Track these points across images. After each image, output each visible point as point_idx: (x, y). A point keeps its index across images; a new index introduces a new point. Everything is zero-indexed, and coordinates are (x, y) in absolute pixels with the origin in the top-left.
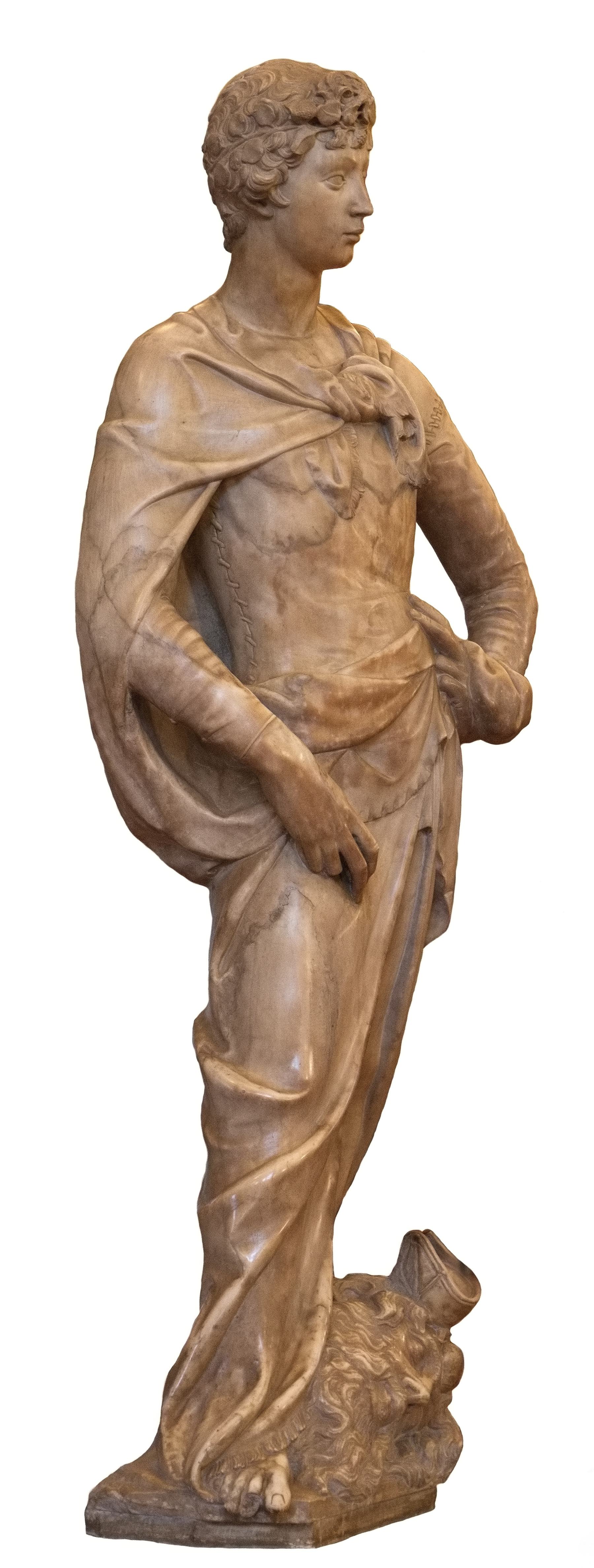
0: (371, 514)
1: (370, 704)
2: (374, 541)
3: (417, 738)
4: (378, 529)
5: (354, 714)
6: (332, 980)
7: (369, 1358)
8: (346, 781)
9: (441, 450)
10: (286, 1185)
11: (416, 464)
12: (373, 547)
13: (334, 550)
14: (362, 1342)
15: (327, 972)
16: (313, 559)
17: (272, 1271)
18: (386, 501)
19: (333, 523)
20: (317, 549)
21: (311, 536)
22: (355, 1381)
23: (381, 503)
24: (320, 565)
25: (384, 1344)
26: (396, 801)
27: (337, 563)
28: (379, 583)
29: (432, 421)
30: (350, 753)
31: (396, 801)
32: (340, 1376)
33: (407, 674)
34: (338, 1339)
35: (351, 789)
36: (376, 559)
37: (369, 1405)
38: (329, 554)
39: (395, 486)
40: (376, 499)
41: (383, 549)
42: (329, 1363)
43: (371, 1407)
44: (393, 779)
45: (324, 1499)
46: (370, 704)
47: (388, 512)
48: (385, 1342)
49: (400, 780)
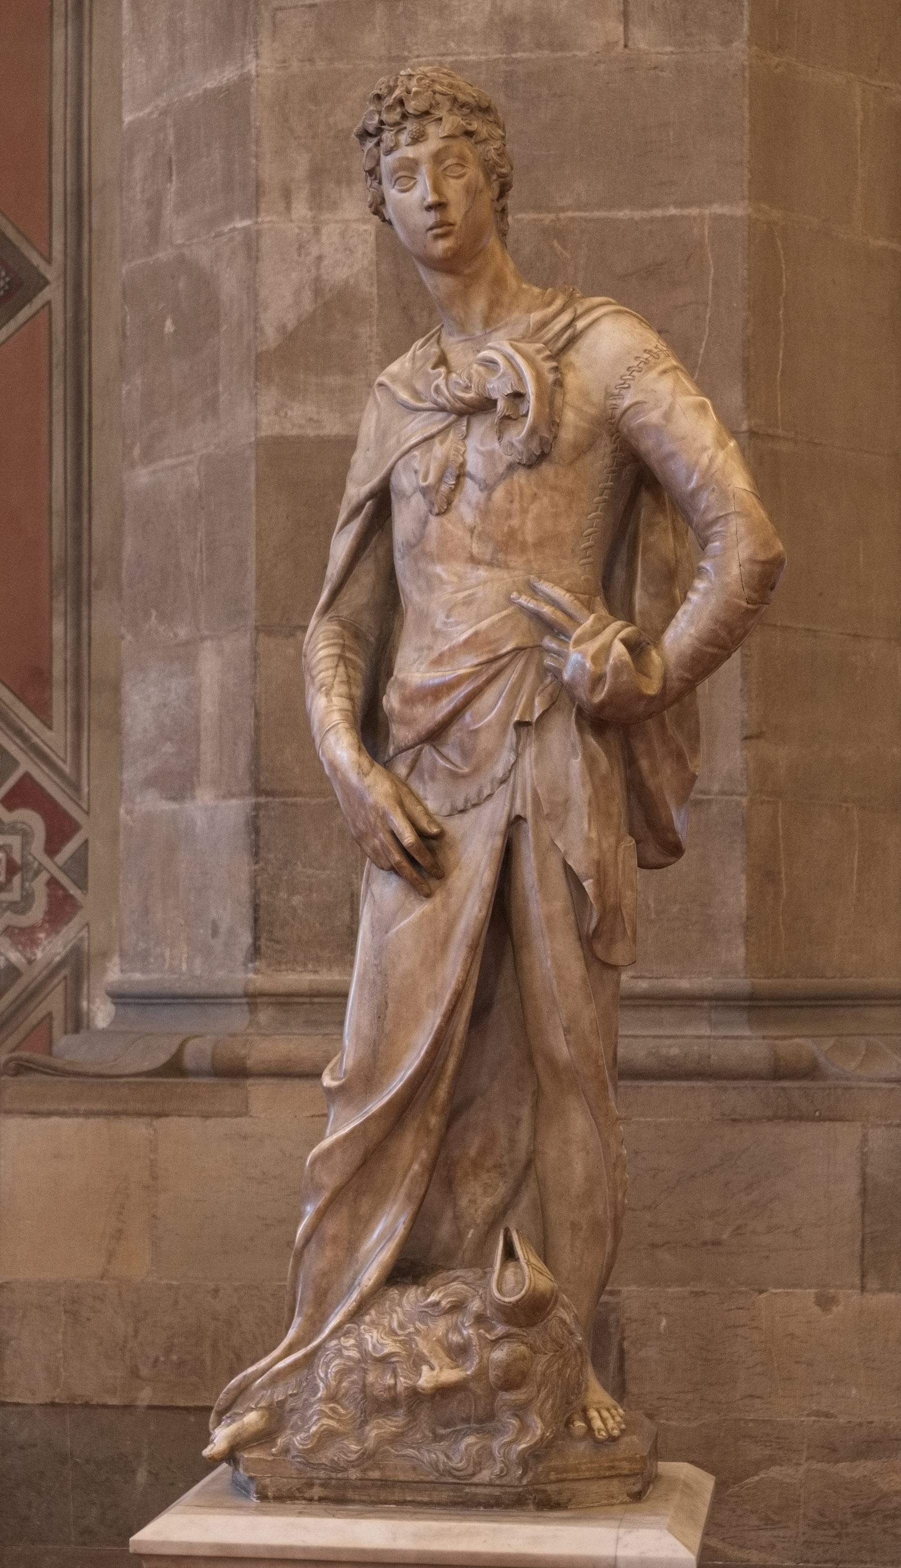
0: (469, 504)
1: (429, 698)
2: (472, 531)
3: (488, 726)
4: (475, 517)
5: (420, 709)
6: (380, 972)
7: (375, 1340)
8: (426, 777)
9: (629, 413)
10: (318, 1166)
11: (520, 442)
12: (471, 537)
13: (428, 549)
14: (386, 1324)
15: (376, 966)
16: (416, 560)
17: (313, 1246)
18: (488, 488)
19: (425, 523)
20: (416, 550)
21: (413, 541)
22: (349, 1358)
23: (481, 490)
24: (422, 565)
25: (412, 1330)
26: (480, 792)
27: (433, 561)
28: (482, 573)
29: (622, 382)
30: (427, 748)
31: (480, 792)
32: (339, 1353)
33: (476, 661)
34: (367, 1318)
35: (430, 784)
36: (476, 548)
37: (361, 1383)
38: (424, 553)
39: (501, 469)
40: (476, 487)
41: (484, 537)
42: (339, 1338)
43: (364, 1386)
44: (466, 770)
45: (270, 1458)
46: (429, 698)
47: (489, 498)
48: (416, 1328)
49: (476, 770)
